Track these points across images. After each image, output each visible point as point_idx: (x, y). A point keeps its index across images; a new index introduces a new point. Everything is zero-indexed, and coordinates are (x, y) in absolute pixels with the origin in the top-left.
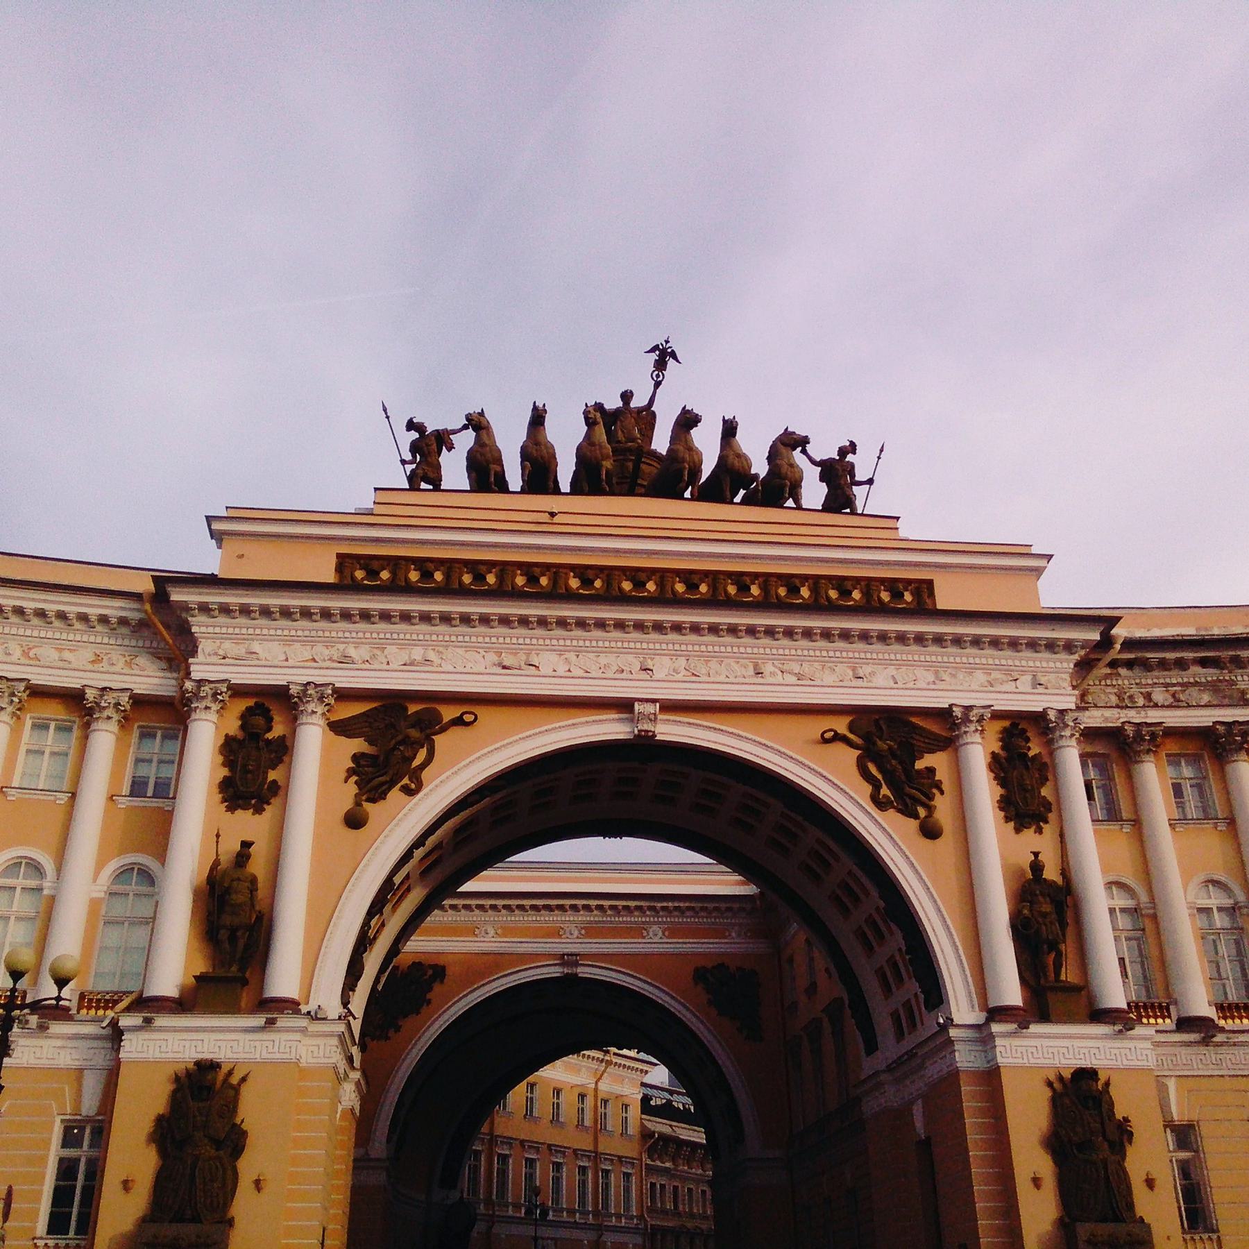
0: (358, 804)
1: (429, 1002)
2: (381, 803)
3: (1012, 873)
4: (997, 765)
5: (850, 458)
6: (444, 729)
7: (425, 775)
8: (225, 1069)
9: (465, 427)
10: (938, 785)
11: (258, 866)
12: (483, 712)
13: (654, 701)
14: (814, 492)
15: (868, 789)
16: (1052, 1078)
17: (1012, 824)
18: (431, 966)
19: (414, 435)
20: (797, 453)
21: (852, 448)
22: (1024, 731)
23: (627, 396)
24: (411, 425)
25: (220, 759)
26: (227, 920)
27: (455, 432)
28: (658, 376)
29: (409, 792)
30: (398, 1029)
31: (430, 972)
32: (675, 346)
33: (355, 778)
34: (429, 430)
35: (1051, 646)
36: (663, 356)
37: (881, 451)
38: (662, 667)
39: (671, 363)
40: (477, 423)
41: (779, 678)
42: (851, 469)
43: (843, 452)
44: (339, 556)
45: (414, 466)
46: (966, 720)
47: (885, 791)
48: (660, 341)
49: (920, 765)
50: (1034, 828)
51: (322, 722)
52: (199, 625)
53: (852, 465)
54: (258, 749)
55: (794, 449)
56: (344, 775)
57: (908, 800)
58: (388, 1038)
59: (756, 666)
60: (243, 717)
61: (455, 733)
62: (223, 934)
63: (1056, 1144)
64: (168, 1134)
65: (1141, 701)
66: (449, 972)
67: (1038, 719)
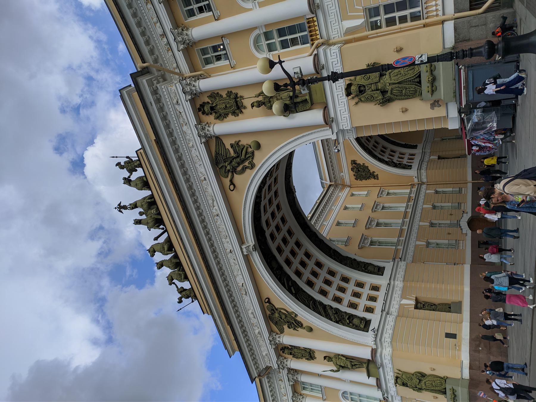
1: (364, 164)
2: (303, 322)
4: (221, 117)
5: (122, 164)
8: (396, 375)
10: (238, 143)
12: (264, 297)
13: (241, 249)
15: (248, 171)
16: (353, 102)
18: (352, 165)
21: (118, 164)
22: (201, 105)
24: (180, 301)
26: (349, 367)
29: (296, 315)
30: (374, 172)
32: (116, 206)
34: (180, 296)
35: (158, 101)
37: (113, 157)
39: (122, 205)
41: (216, 207)
43: (122, 167)
46: (206, 136)
47: (246, 164)
48: (116, 211)
52: (262, 366)
53: (125, 162)
58: (377, 175)
61: (273, 301)
63: (386, 98)
67: (192, 101)
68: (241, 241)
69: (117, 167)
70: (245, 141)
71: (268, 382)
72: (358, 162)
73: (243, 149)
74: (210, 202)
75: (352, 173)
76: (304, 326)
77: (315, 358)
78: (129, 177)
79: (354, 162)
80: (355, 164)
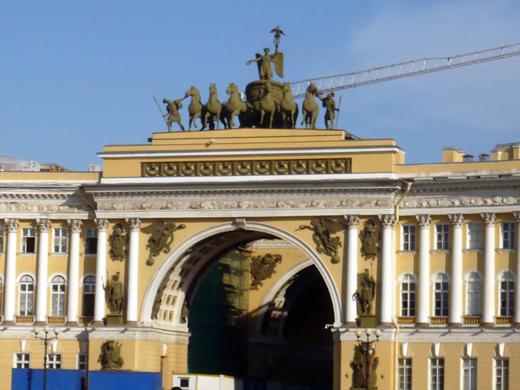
0: (150, 257)
1: (275, 272)
3: (359, 275)
6: (175, 230)
7: (171, 246)
9: (187, 96)
11: (122, 279)
12: (188, 225)
13: (243, 218)
14: (322, 111)
15: (316, 246)
17: (364, 257)
18: (274, 256)
25: (108, 243)
26: (114, 298)
27: (182, 100)
28: (276, 42)
29: (166, 252)
30: (262, 285)
31: (275, 258)
32: (281, 29)
33: (149, 248)
36: (278, 33)
37: (340, 98)
38: (245, 204)
40: (192, 93)
44: (141, 163)
47: (321, 246)
49: (332, 236)
50: (372, 258)
51: (139, 229)
52: (97, 200)
54: (119, 240)
56: (145, 247)
57: (328, 249)
58: (257, 289)
59: (277, 202)
60: (113, 228)
62: (114, 302)
64: (104, 360)
65: (425, 204)
66: (283, 258)
68: (248, 219)
70: (340, 251)
71: (68, 195)
72: (278, 264)
73: (335, 248)
74: (291, 202)
75: (263, 255)
76: (154, 258)
77: (113, 260)
79: (279, 259)
80: (276, 260)
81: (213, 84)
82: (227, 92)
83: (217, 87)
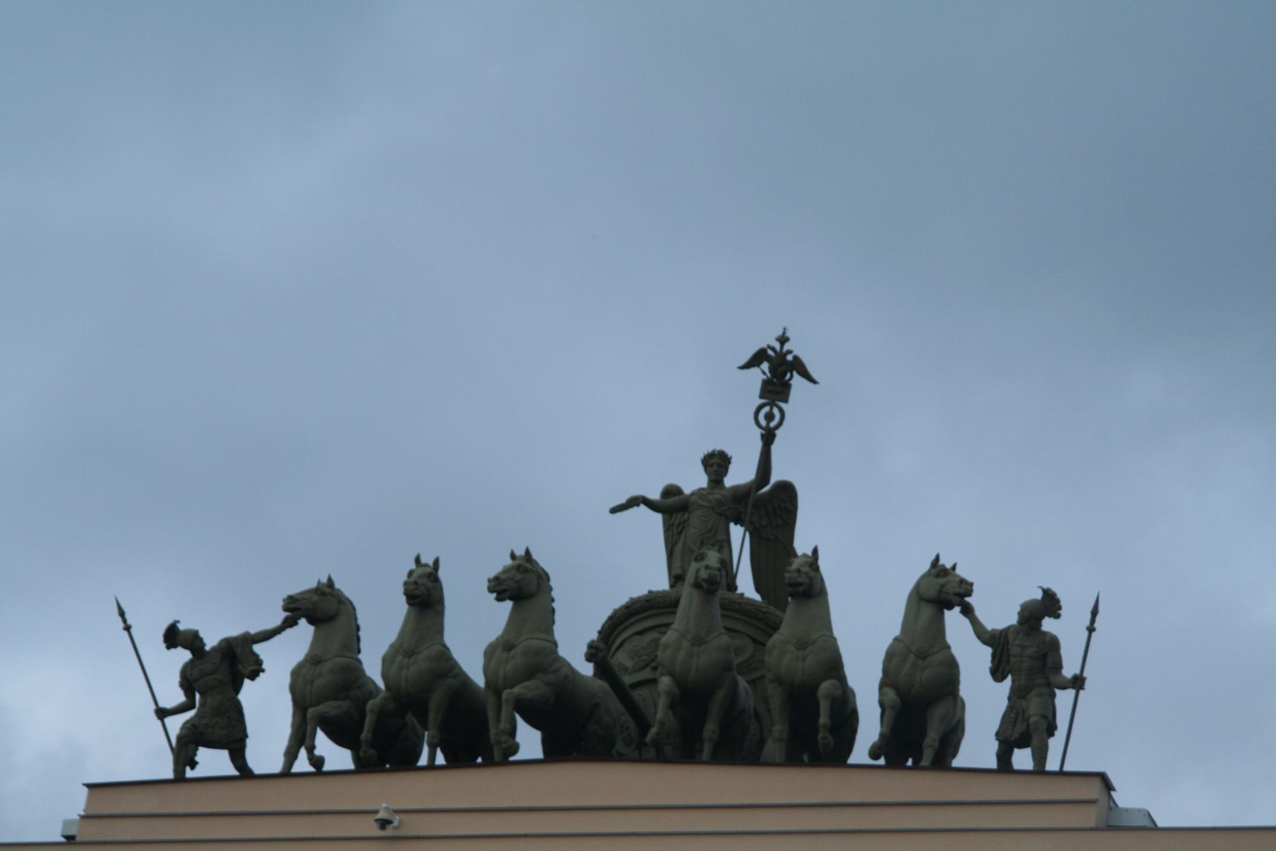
5: (1048, 625)
14: (984, 700)
19: (182, 656)
20: (953, 617)
21: (1049, 604)
23: (717, 463)
24: (173, 637)
28: (770, 417)
32: (795, 347)
34: (211, 642)
36: (779, 371)
37: (1095, 612)
39: (797, 381)
42: (1052, 645)
45: (191, 713)
55: (950, 607)
69: (1038, 595)
78: (968, 611)
81: (428, 559)
82: (500, 588)
83: (442, 574)
